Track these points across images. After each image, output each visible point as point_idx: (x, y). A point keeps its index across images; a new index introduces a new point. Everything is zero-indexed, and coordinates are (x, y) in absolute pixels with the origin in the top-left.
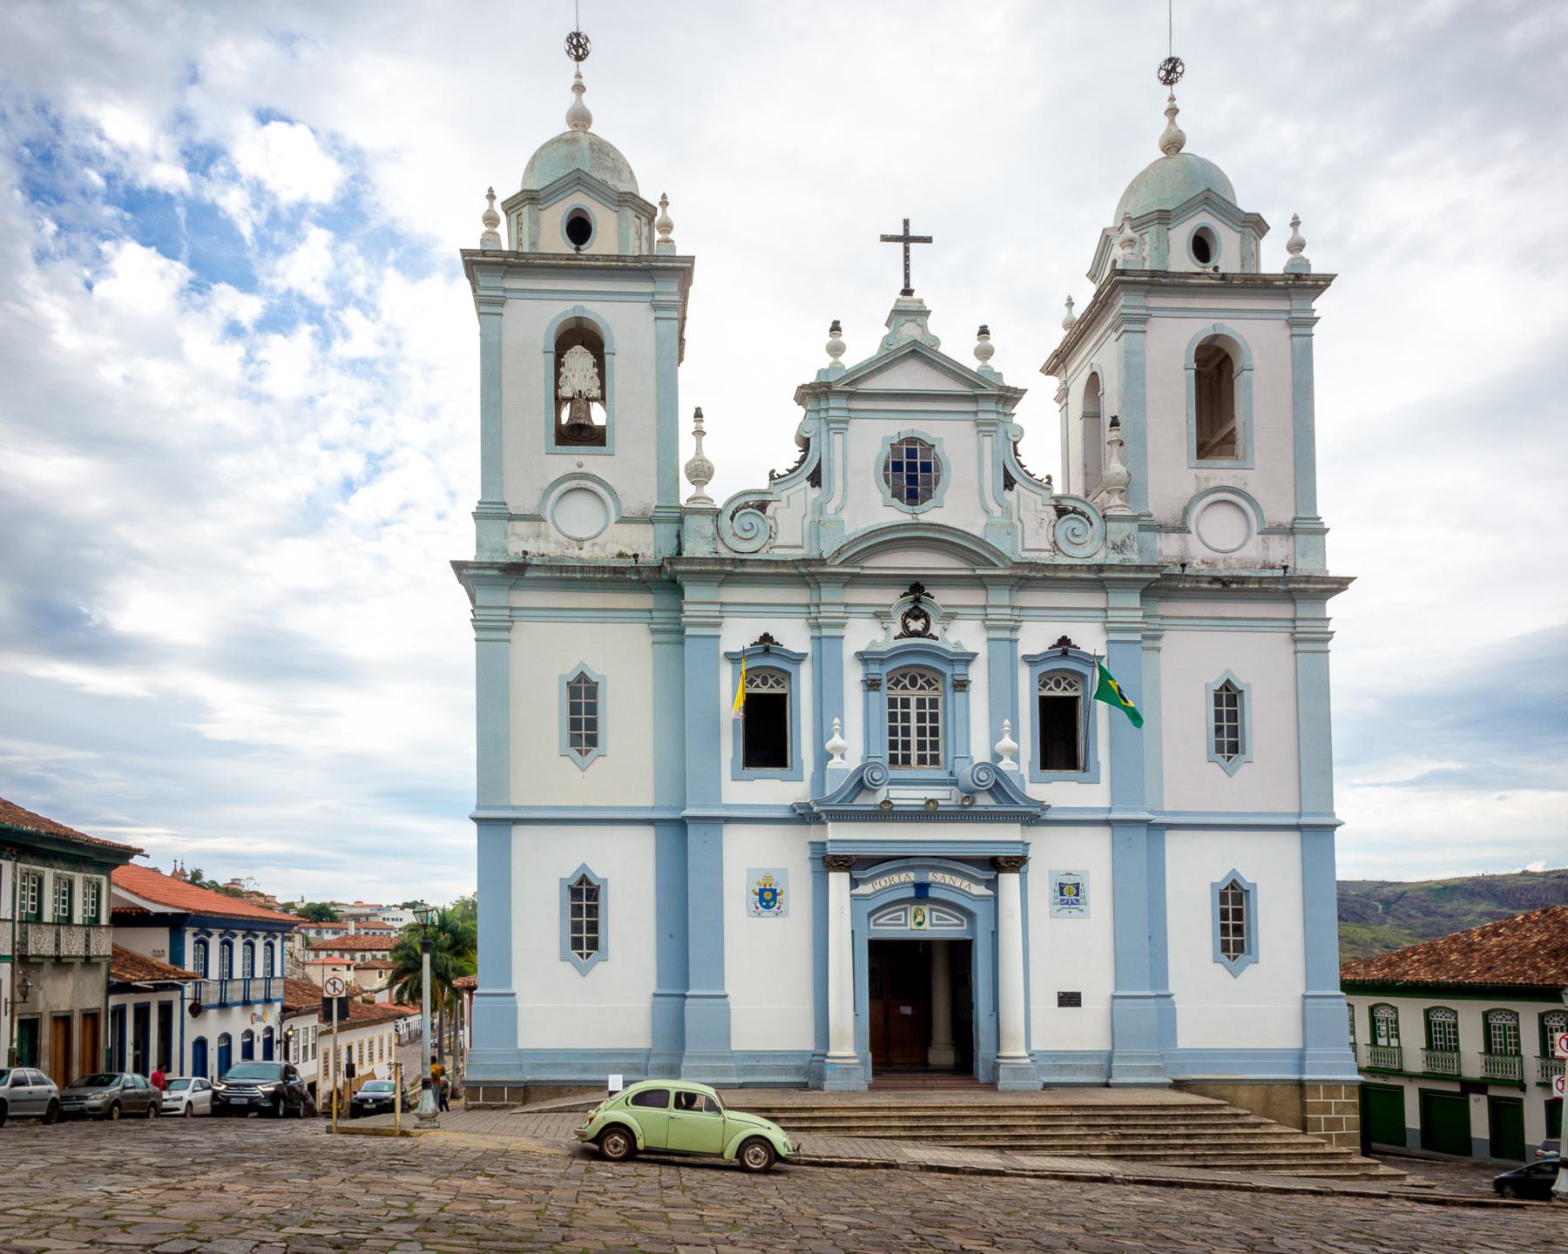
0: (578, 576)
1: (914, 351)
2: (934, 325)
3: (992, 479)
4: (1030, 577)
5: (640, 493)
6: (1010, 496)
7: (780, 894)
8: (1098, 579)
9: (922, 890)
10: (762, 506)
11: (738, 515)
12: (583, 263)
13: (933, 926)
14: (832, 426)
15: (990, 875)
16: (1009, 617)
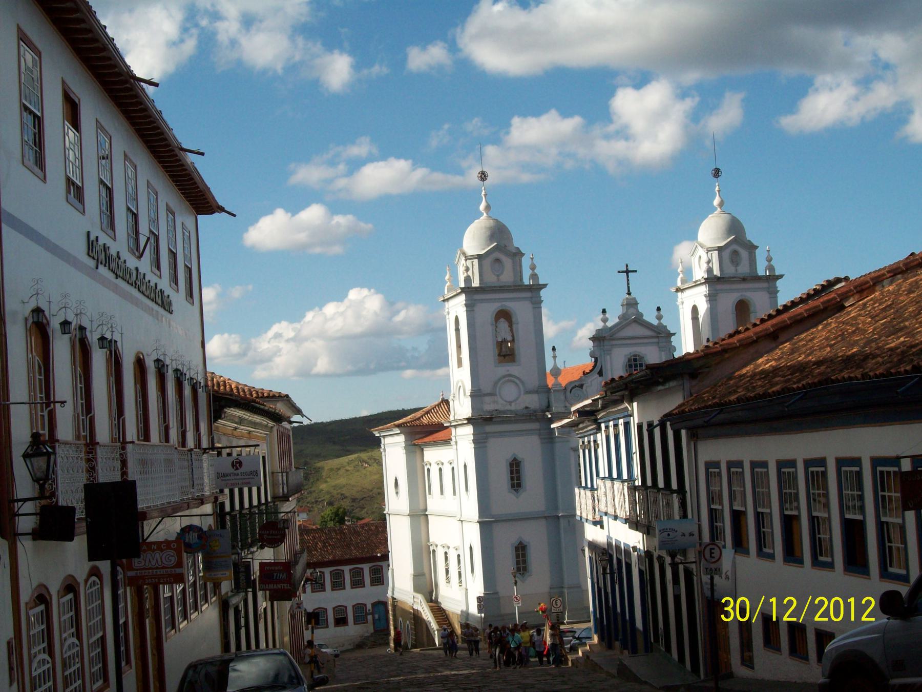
2: (641, 308)
10: (581, 386)
11: (573, 390)
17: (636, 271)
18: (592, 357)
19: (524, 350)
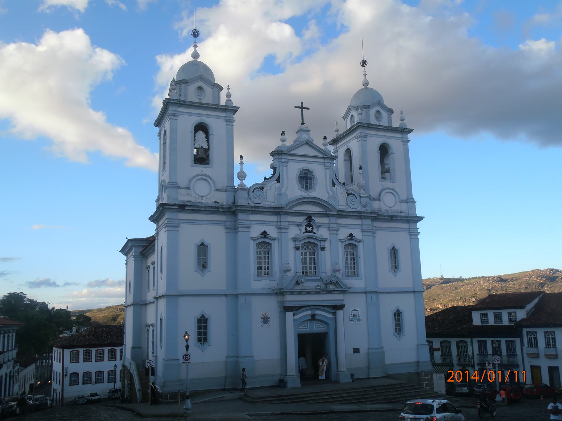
0: (203, 209)
1: (307, 143)
3: (329, 184)
4: (341, 214)
5: (222, 183)
6: (334, 188)
7: (269, 318)
8: (360, 215)
9: (313, 317)
10: (262, 188)
11: (255, 191)
12: (205, 105)
13: (316, 328)
14: (283, 164)
15: (334, 311)
16: (335, 227)
18: (272, 168)
19: (215, 155)
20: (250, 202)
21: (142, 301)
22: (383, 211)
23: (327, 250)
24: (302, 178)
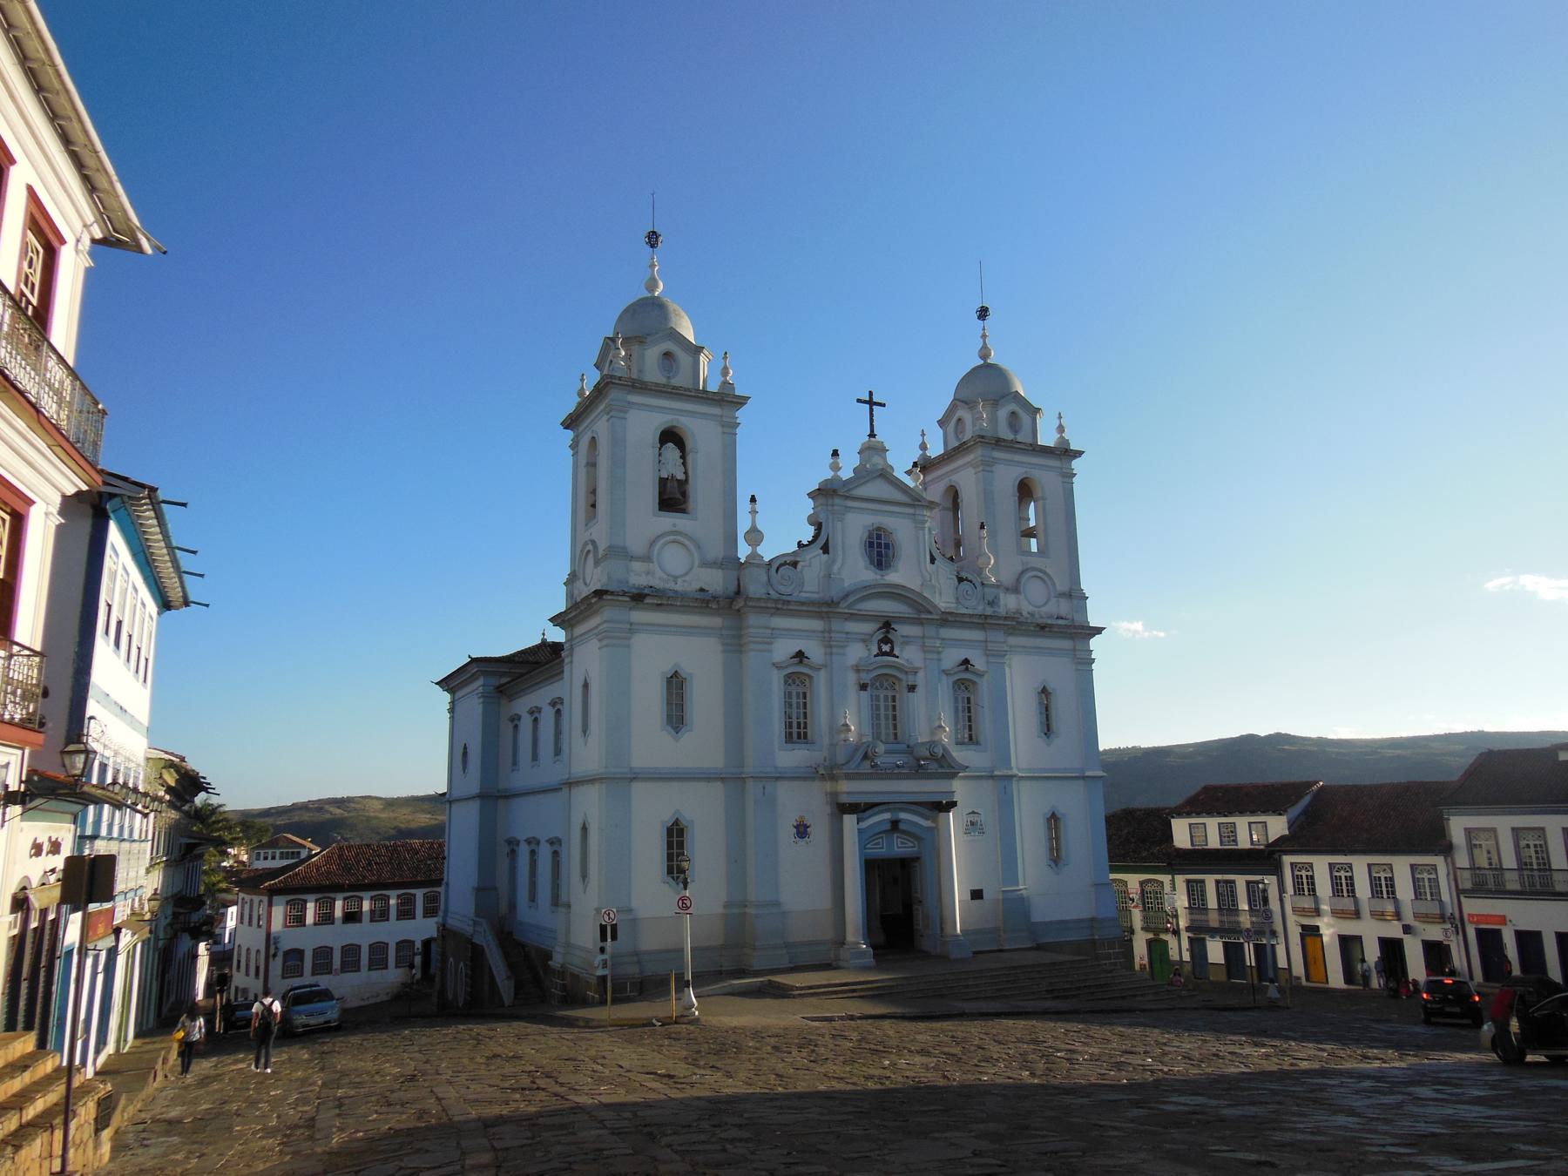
2: (891, 458)
4: (947, 619)
7: (808, 827)
9: (895, 824)
10: (794, 564)
11: (781, 569)
13: (898, 847)
17: (884, 405)
19: (702, 492)
20: (771, 592)
21: (498, 790)
22: (1024, 613)
23: (920, 690)
24: (871, 544)
